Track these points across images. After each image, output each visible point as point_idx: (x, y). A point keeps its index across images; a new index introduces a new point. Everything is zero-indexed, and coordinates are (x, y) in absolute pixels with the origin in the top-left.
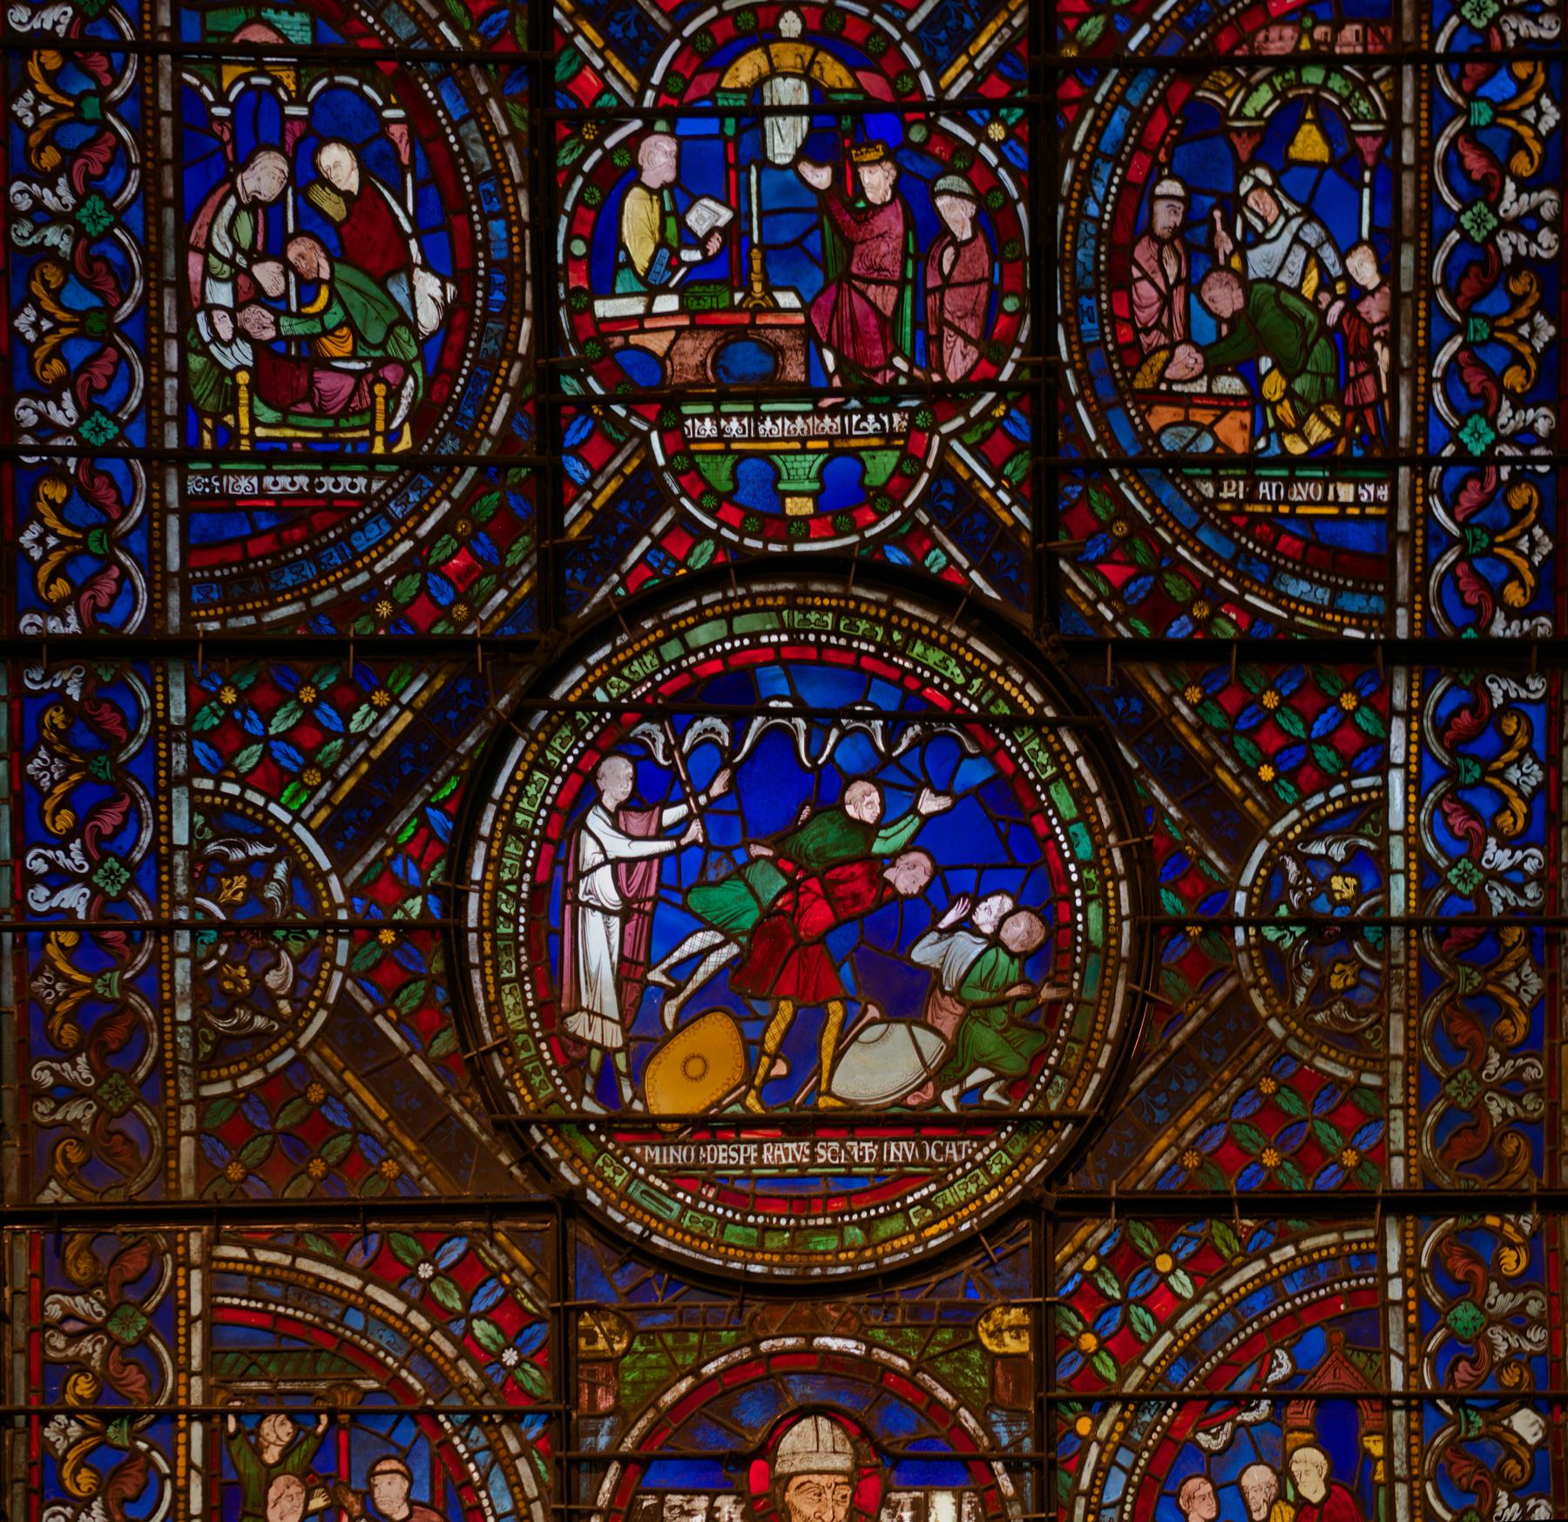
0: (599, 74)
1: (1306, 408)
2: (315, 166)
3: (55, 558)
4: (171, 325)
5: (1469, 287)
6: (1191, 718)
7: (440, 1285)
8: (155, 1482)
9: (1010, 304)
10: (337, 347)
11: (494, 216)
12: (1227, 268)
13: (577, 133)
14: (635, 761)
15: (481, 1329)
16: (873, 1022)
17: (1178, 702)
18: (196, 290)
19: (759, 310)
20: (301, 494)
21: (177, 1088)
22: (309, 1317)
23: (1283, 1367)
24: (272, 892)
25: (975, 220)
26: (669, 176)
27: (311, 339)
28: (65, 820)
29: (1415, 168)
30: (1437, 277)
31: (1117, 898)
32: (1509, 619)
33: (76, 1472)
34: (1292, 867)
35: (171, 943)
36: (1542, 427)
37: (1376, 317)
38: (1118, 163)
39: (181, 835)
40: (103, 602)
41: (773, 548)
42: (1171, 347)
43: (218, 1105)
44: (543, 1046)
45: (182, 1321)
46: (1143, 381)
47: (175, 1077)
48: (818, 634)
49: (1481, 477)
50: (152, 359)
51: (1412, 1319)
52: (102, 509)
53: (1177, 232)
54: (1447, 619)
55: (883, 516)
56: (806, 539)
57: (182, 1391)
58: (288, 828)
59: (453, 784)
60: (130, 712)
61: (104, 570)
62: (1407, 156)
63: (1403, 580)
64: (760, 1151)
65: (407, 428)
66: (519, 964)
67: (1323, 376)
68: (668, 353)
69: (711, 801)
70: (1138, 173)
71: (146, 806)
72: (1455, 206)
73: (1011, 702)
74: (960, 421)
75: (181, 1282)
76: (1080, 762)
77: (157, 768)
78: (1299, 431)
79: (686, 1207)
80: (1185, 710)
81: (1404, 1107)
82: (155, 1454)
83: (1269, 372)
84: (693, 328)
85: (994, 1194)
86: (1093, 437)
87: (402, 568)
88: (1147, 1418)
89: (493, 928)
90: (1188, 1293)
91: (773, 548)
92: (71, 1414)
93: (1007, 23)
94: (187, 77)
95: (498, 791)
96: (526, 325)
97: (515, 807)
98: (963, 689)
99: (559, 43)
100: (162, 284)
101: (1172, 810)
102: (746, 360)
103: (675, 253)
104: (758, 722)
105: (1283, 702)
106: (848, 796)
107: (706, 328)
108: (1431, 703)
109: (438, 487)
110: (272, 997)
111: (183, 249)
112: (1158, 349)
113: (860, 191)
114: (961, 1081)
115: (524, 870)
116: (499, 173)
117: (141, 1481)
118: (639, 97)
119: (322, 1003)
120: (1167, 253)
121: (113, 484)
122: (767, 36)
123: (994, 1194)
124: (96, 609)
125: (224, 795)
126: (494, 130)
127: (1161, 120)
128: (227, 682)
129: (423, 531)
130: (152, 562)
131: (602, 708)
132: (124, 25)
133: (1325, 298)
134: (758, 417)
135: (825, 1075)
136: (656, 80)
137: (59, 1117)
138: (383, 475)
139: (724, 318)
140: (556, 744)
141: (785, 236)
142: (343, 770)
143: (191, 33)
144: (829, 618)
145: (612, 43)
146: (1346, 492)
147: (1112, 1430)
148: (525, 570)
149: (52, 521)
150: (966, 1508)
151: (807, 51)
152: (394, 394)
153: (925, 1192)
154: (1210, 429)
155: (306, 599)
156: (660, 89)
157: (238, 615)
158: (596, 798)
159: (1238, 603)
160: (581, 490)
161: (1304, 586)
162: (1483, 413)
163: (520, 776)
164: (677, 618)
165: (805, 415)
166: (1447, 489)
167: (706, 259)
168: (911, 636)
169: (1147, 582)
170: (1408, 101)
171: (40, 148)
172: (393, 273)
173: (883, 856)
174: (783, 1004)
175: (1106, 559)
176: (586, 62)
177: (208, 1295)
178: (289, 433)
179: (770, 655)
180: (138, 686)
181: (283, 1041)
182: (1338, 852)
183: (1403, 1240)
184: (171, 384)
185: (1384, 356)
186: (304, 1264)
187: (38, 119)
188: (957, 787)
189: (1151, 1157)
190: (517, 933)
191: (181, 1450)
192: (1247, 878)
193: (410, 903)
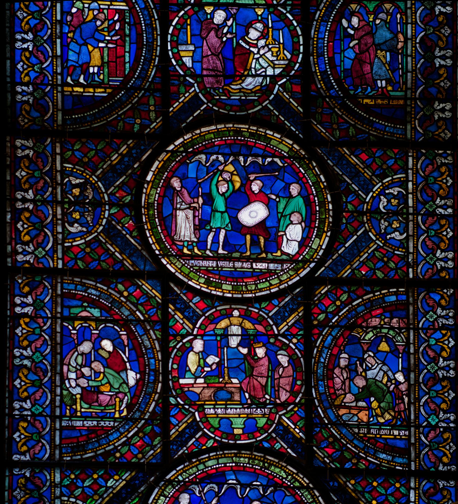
0: (182, 324)
1: (384, 411)
2: (100, 345)
3: (23, 441)
4: (58, 383)
5: (430, 383)
6: (352, 488)
9: (299, 383)
10: (105, 389)
11: (151, 358)
12: (361, 375)
13: (175, 338)
14: (190, 494)
17: (348, 484)
18: (65, 375)
19: (226, 383)
20: (94, 426)
25: (288, 361)
26: (201, 349)
27: (98, 387)
29: (414, 354)
30: (421, 381)
32: (444, 466)
36: (452, 418)
37: (404, 389)
38: (329, 349)
40: (37, 452)
41: (231, 442)
42: (345, 394)
46: (337, 403)
49: (435, 430)
50: (53, 392)
52: (37, 429)
53: (346, 366)
54: (426, 465)
55: (262, 435)
56: (240, 440)
59: (137, 499)
60: (44, 480)
61: (37, 444)
62: (412, 351)
63: (413, 455)
65: (125, 410)
67: (389, 403)
68: (200, 393)
70: (335, 351)
72: (426, 364)
73: (300, 482)
74: (285, 411)
76: (320, 498)
78: (382, 416)
80: (350, 486)
84: (208, 387)
86: (323, 416)
87: (123, 444)
91: (231, 442)
93: (298, 315)
94: (65, 324)
96: (160, 385)
99: (170, 317)
103: (203, 368)
105: (379, 484)
108: (422, 486)
111: (62, 365)
112: (342, 395)
113: (256, 355)
116: (153, 348)
118: (193, 330)
120: (344, 371)
121: (40, 423)
122: (229, 315)
124: (35, 454)
126: (151, 338)
127: (341, 340)
128: (72, 473)
129: (129, 435)
131: (181, 481)
132: (47, 312)
133: (389, 384)
134: (226, 409)
136: (198, 326)
139: (217, 385)
140: (167, 490)
141: (235, 365)
142: (105, 496)
143: (66, 313)
144: (247, 460)
145: (185, 317)
146: (396, 433)
149: (23, 431)
151: (241, 320)
152: (121, 401)
154: (356, 415)
155: (95, 452)
156: (199, 328)
157: (75, 456)
159: (365, 459)
160: (175, 426)
161: (384, 455)
162: (435, 414)
164: (202, 459)
165: (240, 408)
166: (425, 433)
167: (212, 370)
168: (270, 465)
169: (339, 453)
170: (412, 338)
171: (23, 341)
172: (122, 371)
175: (327, 447)
176: (178, 321)
178: (91, 410)
179: (230, 468)
180: (46, 473)
184: (58, 398)
185: (406, 399)
187: (22, 334)
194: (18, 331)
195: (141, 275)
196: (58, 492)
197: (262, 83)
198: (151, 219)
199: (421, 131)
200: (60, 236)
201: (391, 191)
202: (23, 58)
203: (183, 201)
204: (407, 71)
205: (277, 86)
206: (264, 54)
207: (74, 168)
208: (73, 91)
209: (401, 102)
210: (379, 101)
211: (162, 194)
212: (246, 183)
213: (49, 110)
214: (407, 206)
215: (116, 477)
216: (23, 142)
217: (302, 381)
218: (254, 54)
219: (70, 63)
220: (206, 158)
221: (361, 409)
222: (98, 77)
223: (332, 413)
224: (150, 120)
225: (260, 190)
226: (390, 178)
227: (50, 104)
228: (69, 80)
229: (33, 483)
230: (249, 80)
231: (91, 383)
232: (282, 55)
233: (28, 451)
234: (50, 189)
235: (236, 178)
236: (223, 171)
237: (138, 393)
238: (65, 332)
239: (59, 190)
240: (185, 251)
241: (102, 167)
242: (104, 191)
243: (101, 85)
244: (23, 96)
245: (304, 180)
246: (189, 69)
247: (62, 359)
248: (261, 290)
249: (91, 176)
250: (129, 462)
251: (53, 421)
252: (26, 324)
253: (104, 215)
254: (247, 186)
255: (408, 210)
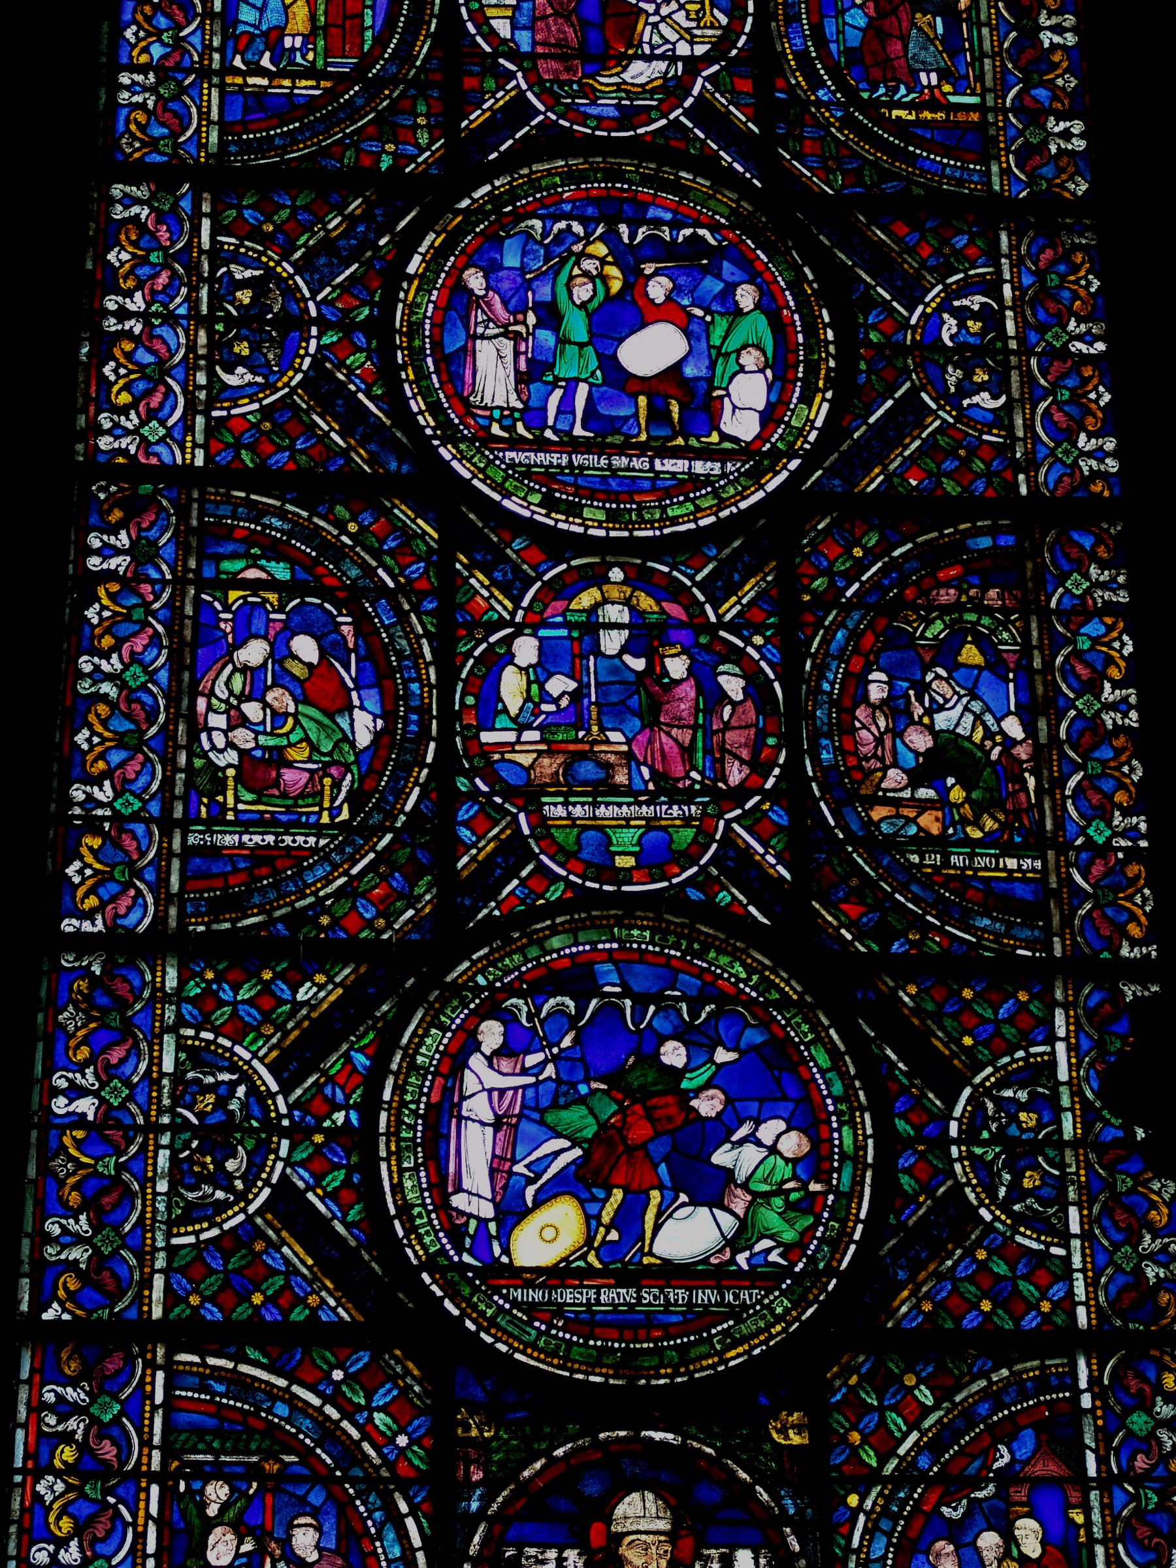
0: (487, 600)
1: (980, 808)
2: (289, 648)
3: (90, 882)
4: (182, 738)
6: (911, 1004)
7: (348, 1385)
8: (119, 1527)
11: (413, 681)
12: (920, 723)
14: (504, 1023)
15: (379, 1418)
16: (684, 1205)
17: (901, 994)
18: (201, 720)
21: (154, 1239)
22: (246, 1407)
23: (1004, 1458)
24: (234, 1106)
26: (534, 660)
27: (280, 749)
28: (84, 1053)
31: (863, 1122)
33: (59, 1518)
34: (990, 1105)
35: (156, 1139)
37: (1024, 757)
39: (168, 1065)
40: (122, 911)
42: (885, 769)
43: (183, 1252)
44: (433, 1216)
45: (147, 1408)
47: (153, 1231)
48: (640, 943)
50: (169, 762)
51: (1100, 1422)
52: (127, 853)
55: (684, 870)
57: (145, 1460)
58: (248, 1063)
59: (371, 1036)
60: (137, 983)
62: (1037, 663)
63: (1056, 920)
64: (598, 1294)
65: (346, 806)
66: (416, 1159)
68: (532, 766)
69: (561, 1050)
70: (857, 664)
71: (144, 1046)
72: (1072, 695)
73: (781, 991)
74: (738, 812)
75: (148, 1379)
76: (832, 1032)
77: (154, 1021)
79: (540, 1333)
80: (906, 999)
81: (1083, 1271)
82: (121, 1507)
83: (953, 786)
84: (550, 753)
85: (778, 1328)
87: (339, 894)
88: (902, 1495)
89: (397, 1133)
90: (929, 1402)
92: (58, 1474)
95: (405, 1041)
96: (432, 745)
97: (416, 1052)
98: (745, 981)
99: (459, 582)
100: (178, 715)
101: (901, 1065)
102: (587, 770)
104: (594, 1003)
106: (662, 1050)
107: (558, 752)
109: (366, 843)
110: (230, 1177)
111: (194, 695)
113: (666, 673)
114: (751, 1247)
115: (421, 1094)
116: (418, 654)
117: (109, 1526)
118: (513, 614)
119: (267, 1182)
121: (134, 837)
122: (600, 580)
123: (778, 1328)
124: (117, 916)
125: (202, 1040)
126: (413, 631)
130: (159, 887)
131: (483, 989)
132: (164, 567)
133: (988, 743)
135: (647, 1242)
136: (525, 603)
137: (63, 1257)
138: (328, 835)
139: (572, 747)
142: (290, 1025)
143: (208, 572)
145: (494, 583)
146: (1012, 863)
147: (875, 1503)
148: (428, 897)
149: (89, 859)
150: (762, 1561)
151: (629, 591)
152: (336, 785)
153: (725, 1326)
155: (269, 913)
157: (219, 922)
158: (477, 1046)
159: (941, 931)
160: (468, 848)
162: (1102, 819)
163: (420, 1032)
164: (537, 931)
171: (102, 636)
172: (340, 711)
173: (688, 1091)
174: (615, 1191)
175: (846, 900)
176: (477, 592)
177: (168, 1387)
178: (262, 808)
179: (605, 956)
180: (144, 966)
181: (236, 1209)
182: (1023, 1096)
183: (1089, 1365)
185: (1031, 782)
186: (244, 1368)
187: (101, 619)
188: (743, 1044)
189: (896, 1303)
190: (415, 1137)
191: (142, 1505)
192: (958, 1112)
193: (335, 1116)
196: (170, 1015)
197: (667, 72)
198: (416, 356)
199: (1023, 177)
200: (202, 395)
201: (966, 302)
202: (139, 17)
203: (490, 320)
204: (983, 55)
205: (700, 81)
206: (669, 16)
207: (242, 245)
208: (246, 85)
209: (975, 117)
210: (927, 115)
211: (442, 304)
212: (635, 280)
213: (190, 123)
214: (1003, 336)
215: (320, 978)
216: (127, 189)
217: (778, 736)
218: (648, 15)
219: (242, 28)
220: (544, 227)
221: (924, 806)
222: (303, 57)
223: (854, 817)
224: (417, 145)
225: (668, 298)
226: (961, 276)
227: (194, 110)
228: (238, 62)
229: (110, 993)
230: (637, 67)
231: (262, 739)
232: (708, 18)
233: (101, 908)
234: (184, 290)
235: (612, 271)
237: (377, 765)
238: (205, 618)
239: (204, 293)
240: (496, 429)
241: (305, 245)
242: (307, 295)
244: (134, 93)
245: (767, 276)
246: (505, 41)
247: (195, 682)
248: (674, 521)
249: (278, 263)
250: (353, 939)
251: (167, 834)
252: (111, 596)
253: (306, 348)
254: (638, 288)
255: (1006, 344)
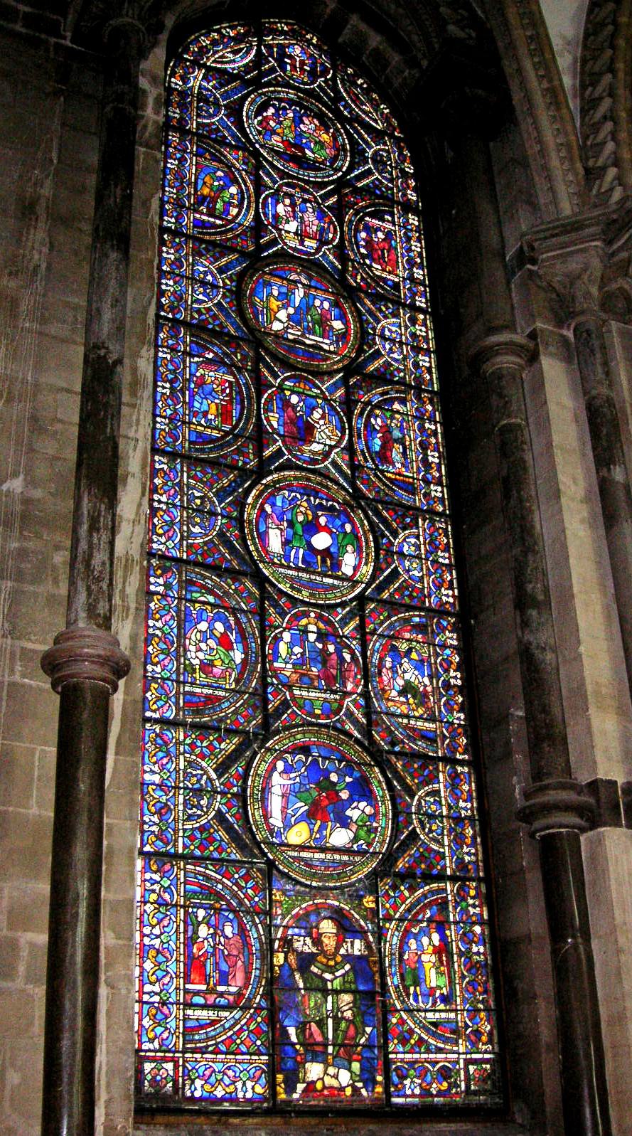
10: (218, 663)
111: (185, 638)
143: (189, 597)
152: (230, 675)
194: (152, 605)
195: (244, 574)
212: (316, 517)
228: (194, 420)
235: (309, 512)
236: (300, 505)
238: (188, 614)
240: (276, 560)
243: (216, 428)
247: (185, 634)
